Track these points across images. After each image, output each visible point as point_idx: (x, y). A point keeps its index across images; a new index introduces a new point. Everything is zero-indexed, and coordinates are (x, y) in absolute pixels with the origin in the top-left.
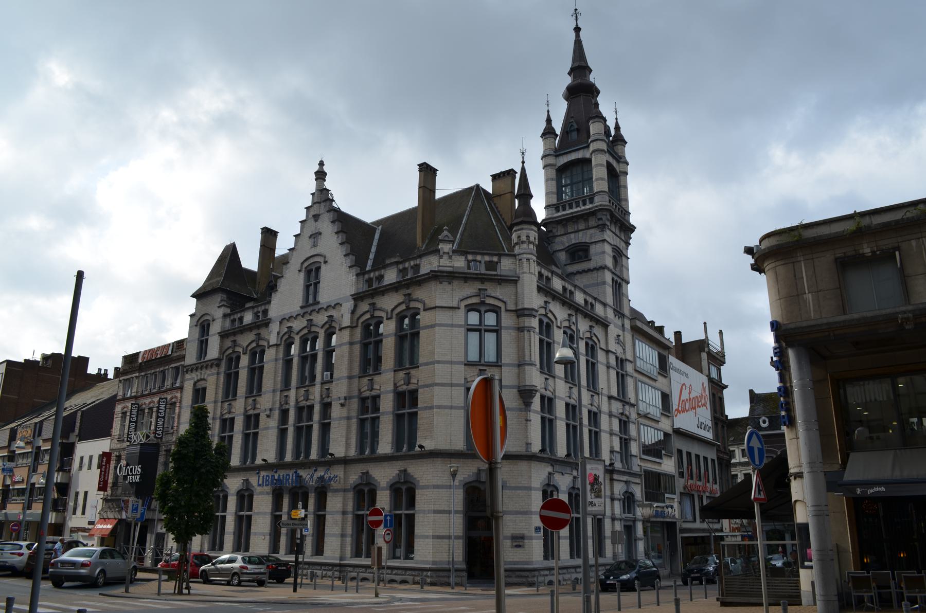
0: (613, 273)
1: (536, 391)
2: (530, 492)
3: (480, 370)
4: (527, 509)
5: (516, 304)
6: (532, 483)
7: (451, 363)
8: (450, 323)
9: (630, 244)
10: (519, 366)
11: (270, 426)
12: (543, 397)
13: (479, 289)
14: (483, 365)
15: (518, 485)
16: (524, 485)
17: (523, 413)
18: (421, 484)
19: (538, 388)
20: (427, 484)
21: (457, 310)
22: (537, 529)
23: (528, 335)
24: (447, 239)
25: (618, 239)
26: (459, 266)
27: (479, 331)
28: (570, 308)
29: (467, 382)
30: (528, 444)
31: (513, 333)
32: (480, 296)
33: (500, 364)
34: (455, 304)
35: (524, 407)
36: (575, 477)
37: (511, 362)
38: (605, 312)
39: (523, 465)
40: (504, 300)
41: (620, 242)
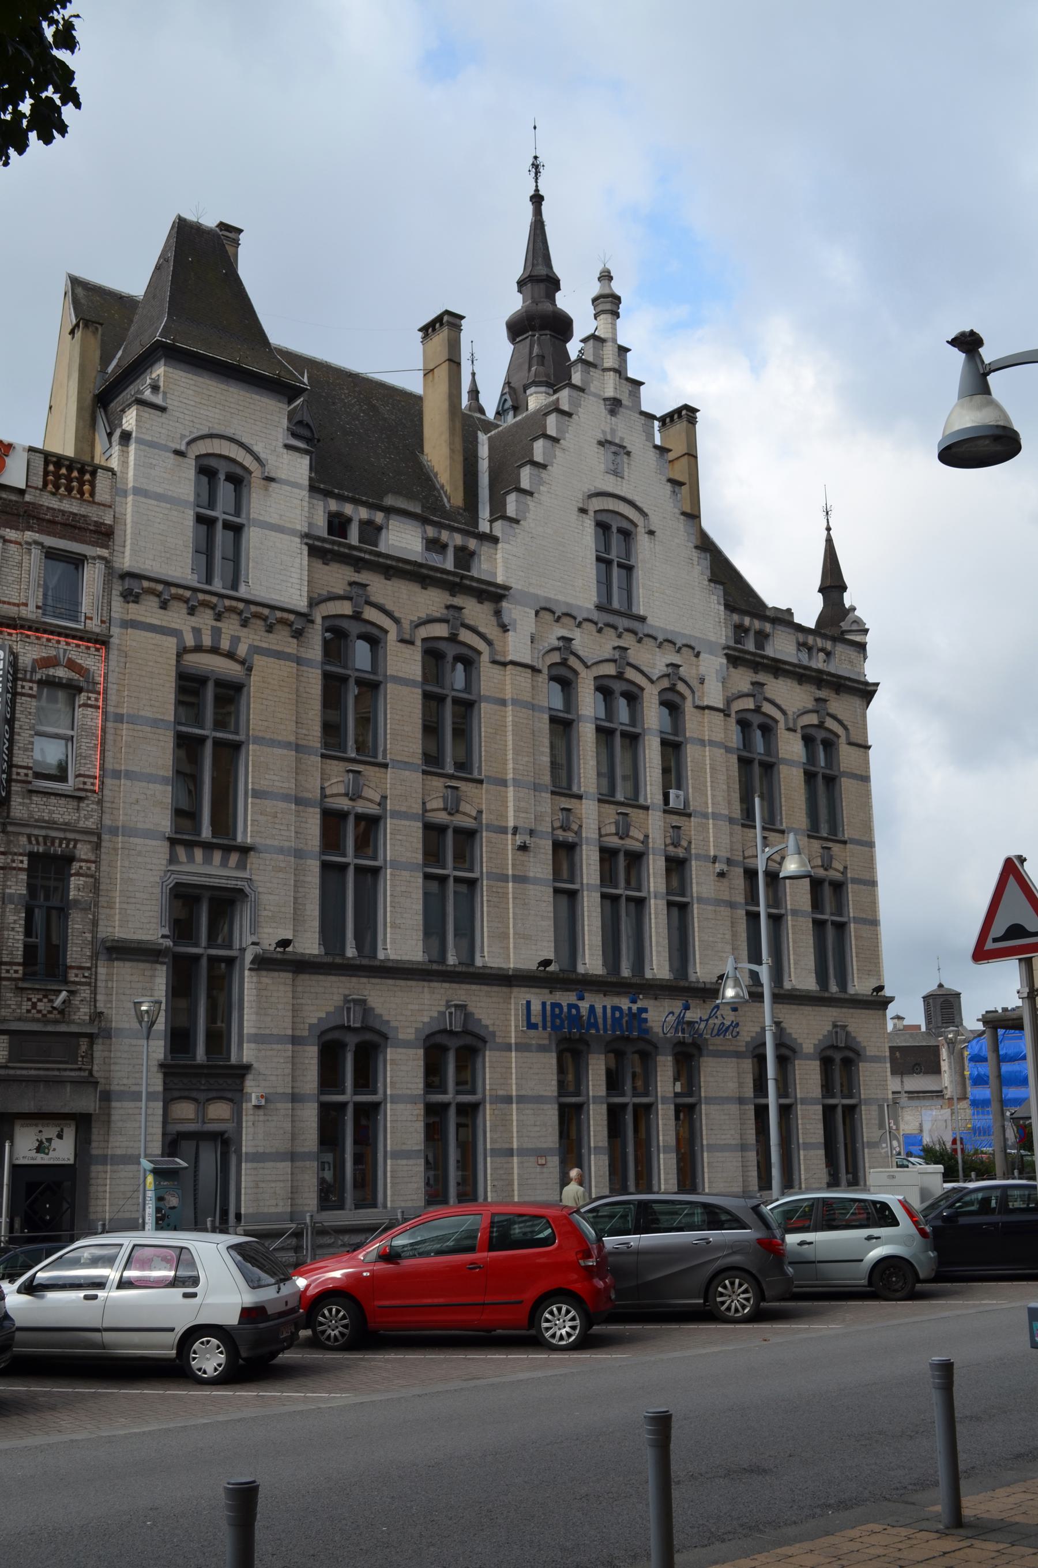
11: (531, 874)
18: (868, 1054)
20: (877, 1054)
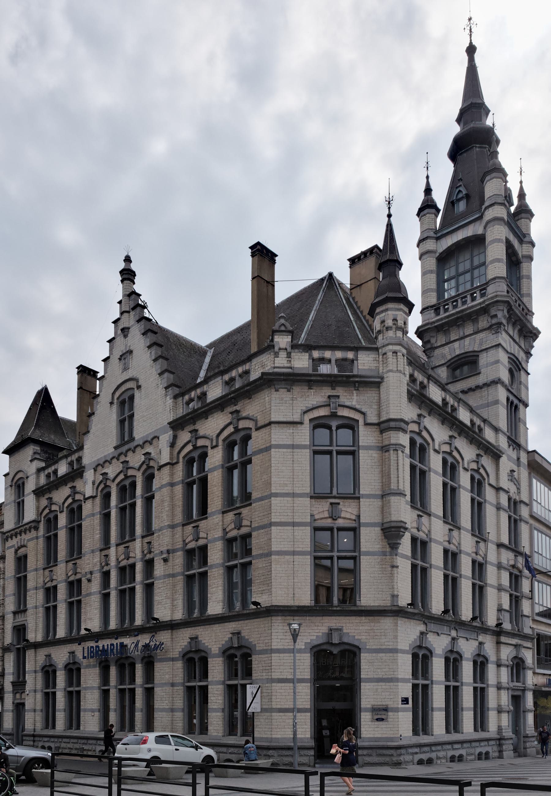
0: (508, 390)
1: (406, 529)
2: (395, 655)
3: (331, 504)
4: (393, 676)
5: (379, 415)
6: (399, 644)
7: (293, 495)
8: (290, 442)
9: (531, 355)
10: (383, 496)
12: (414, 540)
13: (329, 397)
14: (335, 497)
15: (378, 647)
16: (388, 647)
17: (388, 557)
19: (408, 526)
21: (299, 426)
22: (405, 701)
23: (395, 456)
24: (283, 328)
25: (517, 347)
26: (301, 366)
27: (330, 453)
28: (451, 428)
29: (315, 520)
30: (394, 597)
31: (375, 454)
32: (329, 405)
33: (357, 495)
34: (296, 418)
35: (388, 550)
36: (453, 639)
37: (371, 493)
38: (497, 439)
39: (387, 622)
40: (363, 410)
41: (519, 351)
